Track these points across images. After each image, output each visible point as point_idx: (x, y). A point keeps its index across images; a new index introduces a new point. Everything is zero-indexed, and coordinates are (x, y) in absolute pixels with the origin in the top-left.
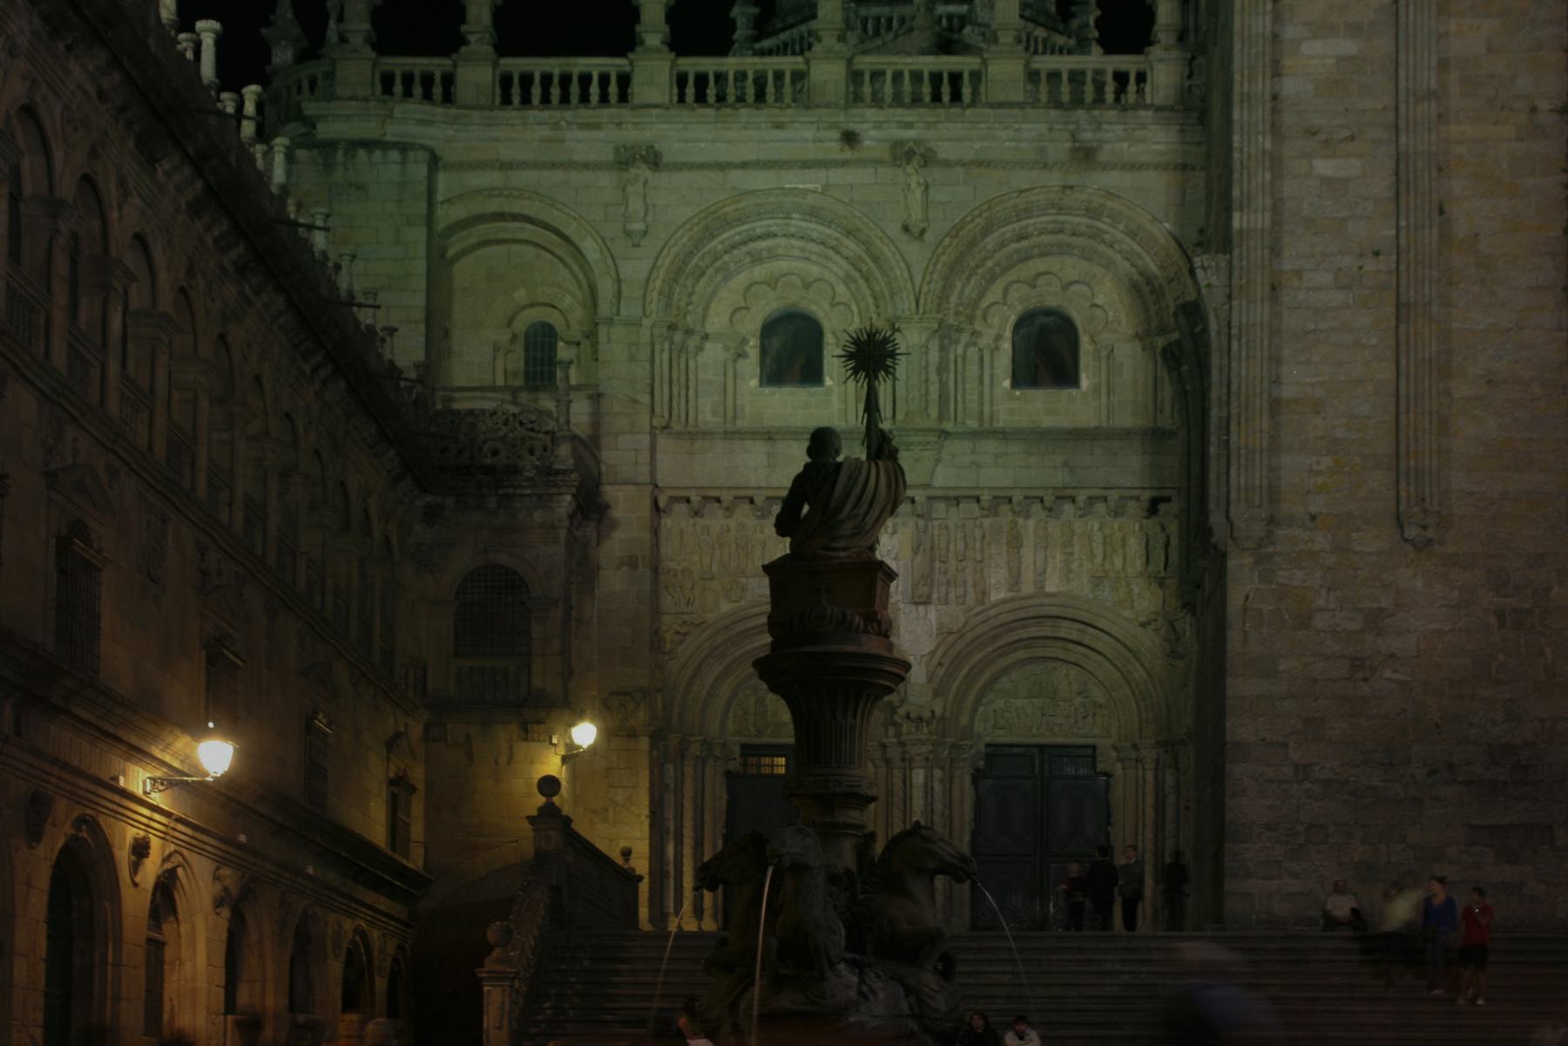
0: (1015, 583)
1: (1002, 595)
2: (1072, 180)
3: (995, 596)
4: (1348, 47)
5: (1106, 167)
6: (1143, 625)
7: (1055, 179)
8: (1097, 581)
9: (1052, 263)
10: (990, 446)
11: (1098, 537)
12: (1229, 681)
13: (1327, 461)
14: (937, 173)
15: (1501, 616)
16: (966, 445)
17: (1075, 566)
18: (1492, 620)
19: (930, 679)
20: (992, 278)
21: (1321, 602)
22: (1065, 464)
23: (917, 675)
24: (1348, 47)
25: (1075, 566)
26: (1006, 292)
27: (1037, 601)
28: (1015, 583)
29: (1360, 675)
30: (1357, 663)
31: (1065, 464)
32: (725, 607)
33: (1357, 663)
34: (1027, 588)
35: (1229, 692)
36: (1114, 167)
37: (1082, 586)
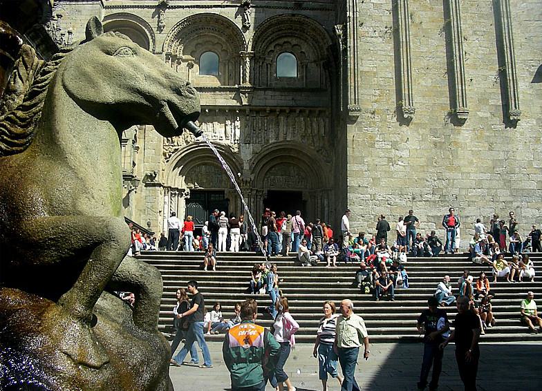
1: (273, 141)
2: (295, 12)
5: (305, 9)
6: (318, 151)
7: (290, 12)
8: (303, 137)
10: (270, 93)
11: (303, 123)
15: (435, 144)
16: (263, 92)
17: (296, 132)
21: (377, 139)
26: (274, 47)
27: (284, 143)
28: (277, 138)
29: (391, 164)
30: (390, 160)
31: (293, 99)
33: (390, 160)
34: (281, 139)
37: (298, 139)
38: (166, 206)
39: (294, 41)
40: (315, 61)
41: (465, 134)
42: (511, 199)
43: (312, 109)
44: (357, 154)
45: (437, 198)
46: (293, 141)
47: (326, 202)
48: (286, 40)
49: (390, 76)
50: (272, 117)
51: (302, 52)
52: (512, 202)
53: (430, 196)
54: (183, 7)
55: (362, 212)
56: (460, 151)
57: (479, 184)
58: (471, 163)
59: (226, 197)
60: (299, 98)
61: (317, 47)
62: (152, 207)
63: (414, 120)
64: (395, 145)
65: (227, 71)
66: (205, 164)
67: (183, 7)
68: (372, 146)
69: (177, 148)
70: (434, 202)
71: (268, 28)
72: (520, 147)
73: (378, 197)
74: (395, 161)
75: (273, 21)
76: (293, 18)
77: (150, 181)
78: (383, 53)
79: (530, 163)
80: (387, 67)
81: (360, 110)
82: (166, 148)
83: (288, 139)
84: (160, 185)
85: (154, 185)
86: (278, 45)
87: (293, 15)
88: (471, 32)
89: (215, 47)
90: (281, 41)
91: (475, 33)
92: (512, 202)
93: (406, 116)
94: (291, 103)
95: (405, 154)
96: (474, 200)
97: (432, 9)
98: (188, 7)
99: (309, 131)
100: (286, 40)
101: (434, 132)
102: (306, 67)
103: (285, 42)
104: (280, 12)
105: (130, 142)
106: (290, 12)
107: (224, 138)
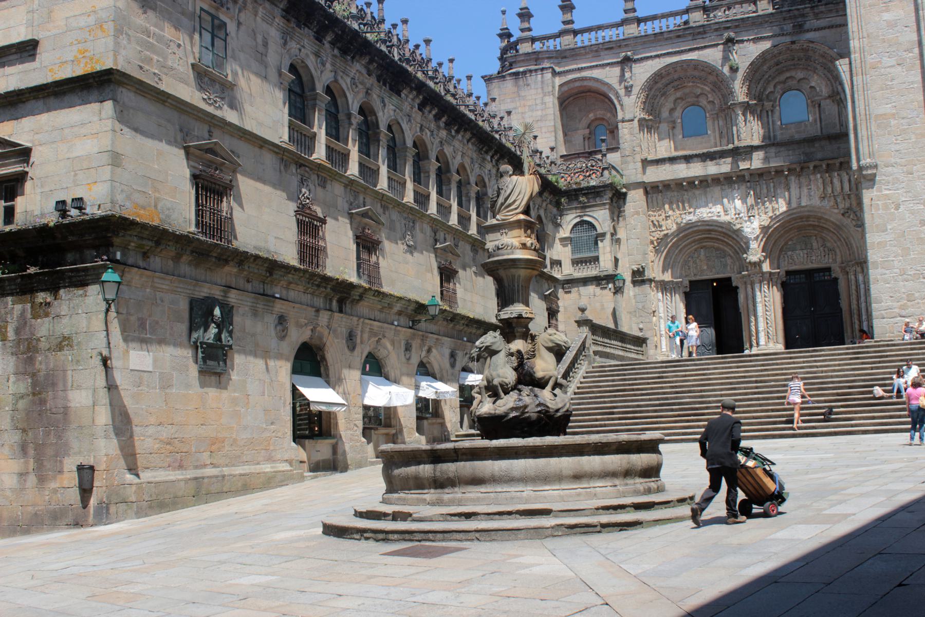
2: (794, 39)
5: (808, 31)
7: (788, 39)
8: (823, 198)
9: (793, 73)
11: (820, 181)
12: (867, 236)
17: (812, 193)
20: (768, 82)
23: (754, 245)
26: (775, 86)
34: (794, 205)
36: (811, 30)
37: (816, 202)
38: (661, 304)
39: (800, 74)
40: (829, 97)
43: (830, 162)
48: (788, 75)
51: (811, 87)
61: (830, 77)
65: (717, 129)
69: (665, 232)
76: (794, 46)
77: (639, 277)
82: (653, 234)
83: (803, 204)
86: (780, 83)
90: (782, 77)
99: (829, 190)
100: (788, 75)
102: (819, 105)
103: (787, 78)
105: (608, 236)
107: (722, 213)
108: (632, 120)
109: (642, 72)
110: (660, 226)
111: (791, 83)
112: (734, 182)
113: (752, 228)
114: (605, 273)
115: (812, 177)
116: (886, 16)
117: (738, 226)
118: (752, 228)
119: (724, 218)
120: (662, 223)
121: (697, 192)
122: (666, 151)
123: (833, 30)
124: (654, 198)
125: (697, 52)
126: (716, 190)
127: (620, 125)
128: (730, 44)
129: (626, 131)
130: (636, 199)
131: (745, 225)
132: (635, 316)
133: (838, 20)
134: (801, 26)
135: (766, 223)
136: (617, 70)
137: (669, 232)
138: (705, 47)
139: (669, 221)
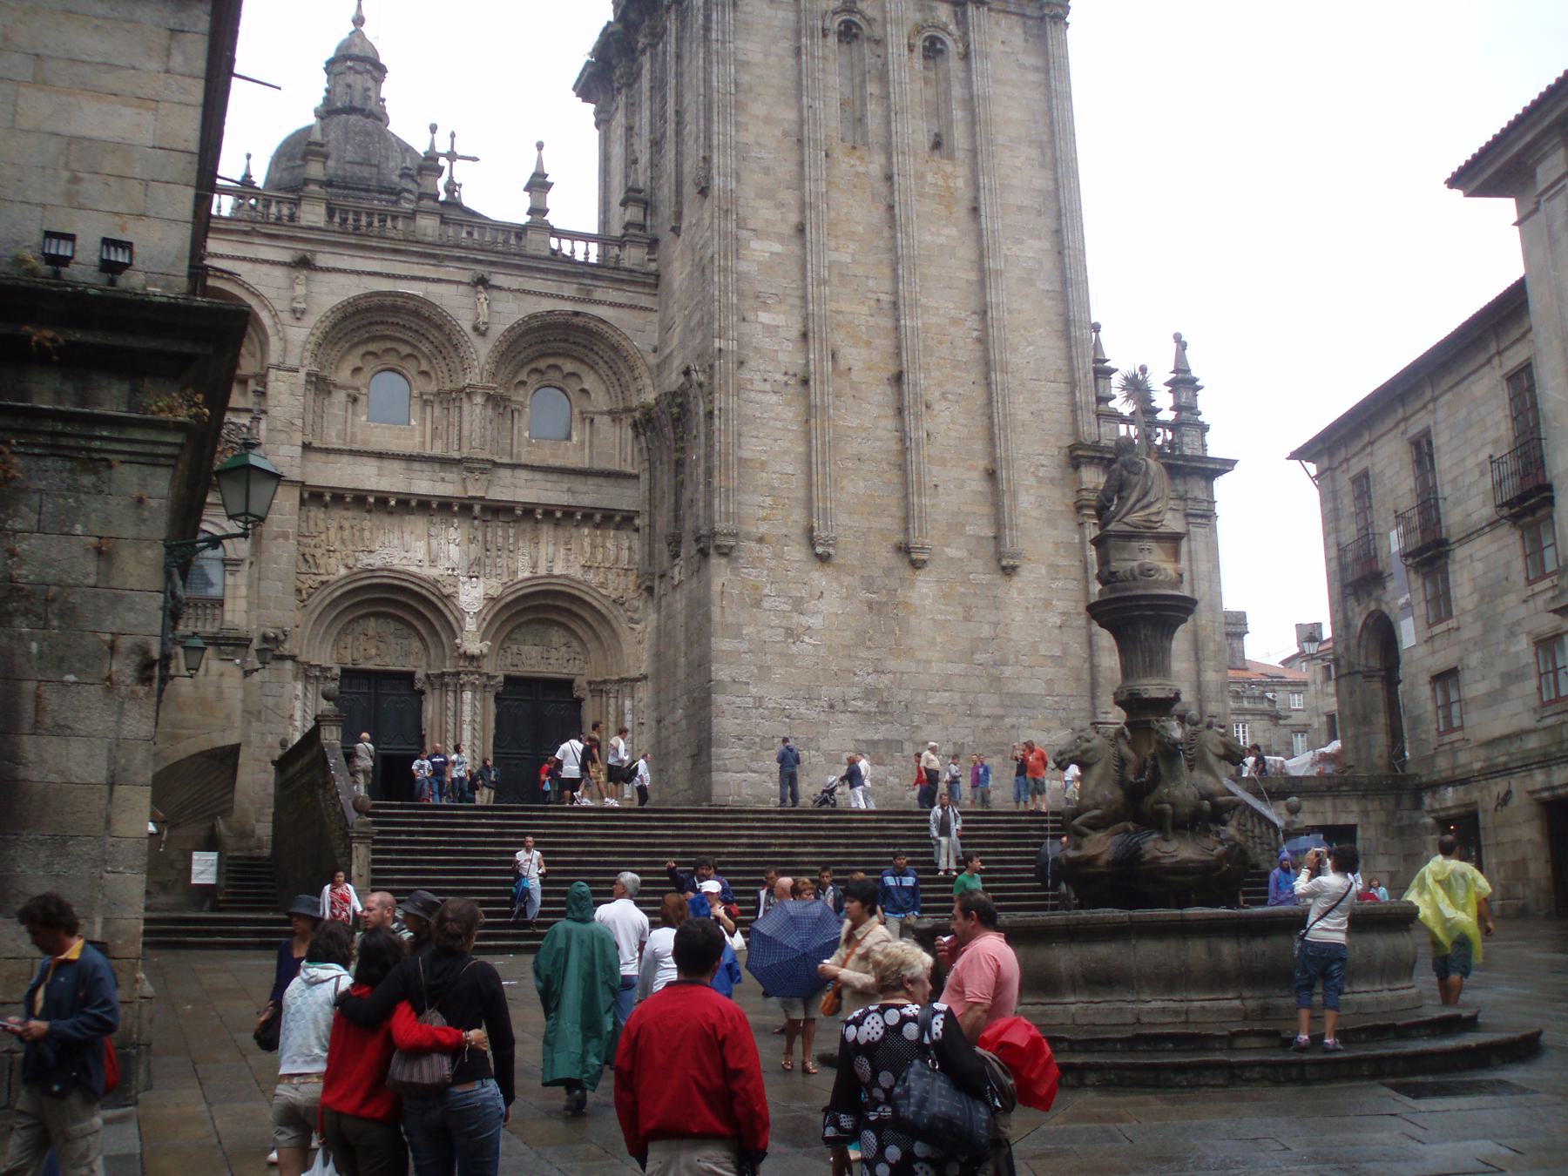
0: (535, 566)
1: (527, 574)
3: (521, 576)
4: (777, 248)
13: (769, 501)
14: (496, 293)
15: (870, 605)
17: (572, 558)
18: (865, 608)
19: (479, 628)
21: (766, 591)
22: (569, 490)
23: (470, 625)
24: (777, 248)
25: (572, 558)
28: (535, 566)
31: (569, 490)
32: (343, 571)
34: (542, 571)
35: (713, 646)
37: (576, 572)
41: (924, 589)
42: (999, 711)
44: (730, 619)
45: (871, 707)
46: (566, 577)
47: (628, 703)
49: (790, 470)
50: (527, 526)
52: (1002, 717)
53: (860, 703)
54: (345, 271)
55: (738, 731)
56: (913, 620)
57: (946, 684)
58: (933, 643)
59: (418, 686)
60: (584, 489)
62: (276, 705)
63: (838, 560)
64: (798, 605)
66: (377, 615)
67: (345, 271)
68: (758, 604)
69: (324, 578)
70: (868, 714)
71: (522, 335)
72: (1018, 616)
73: (766, 703)
74: (798, 636)
75: (535, 324)
78: (779, 424)
79: (1034, 645)
80: (786, 453)
81: (736, 535)
82: (303, 578)
83: (556, 572)
84: (293, 658)
85: (282, 658)
86: (536, 370)
87: (576, 314)
88: (937, 394)
89: (404, 364)
91: (944, 396)
92: (1002, 717)
93: (819, 550)
94: (565, 499)
95: (815, 622)
96: (936, 711)
97: (868, 344)
98: (358, 273)
99: (600, 557)
101: (868, 583)
103: (549, 367)
104: (547, 305)
106: (569, 307)
108: (296, 371)
109: (332, 291)
110: (317, 566)
111: (554, 375)
112: (454, 515)
113: (471, 597)
114: (232, 634)
115: (574, 531)
116: (764, 317)
117: (447, 591)
118: (471, 597)
119: (428, 572)
120: (321, 562)
121: (387, 520)
122: (338, 437)
123: (636, 313)
124: (312, 514)
125: (423, 285)
126: (419, 524)
127: (273, 374)
128: (480, 288)
129: (283, 387)
130: (286, 503)
131: (461, 589)
132: (259, 719)
133: (645, 301)
134: (589, 292)
135: (495, 592)
136: (279, 272)
137: (332, 578)
138: (439, 281)
139: (333, 561)
